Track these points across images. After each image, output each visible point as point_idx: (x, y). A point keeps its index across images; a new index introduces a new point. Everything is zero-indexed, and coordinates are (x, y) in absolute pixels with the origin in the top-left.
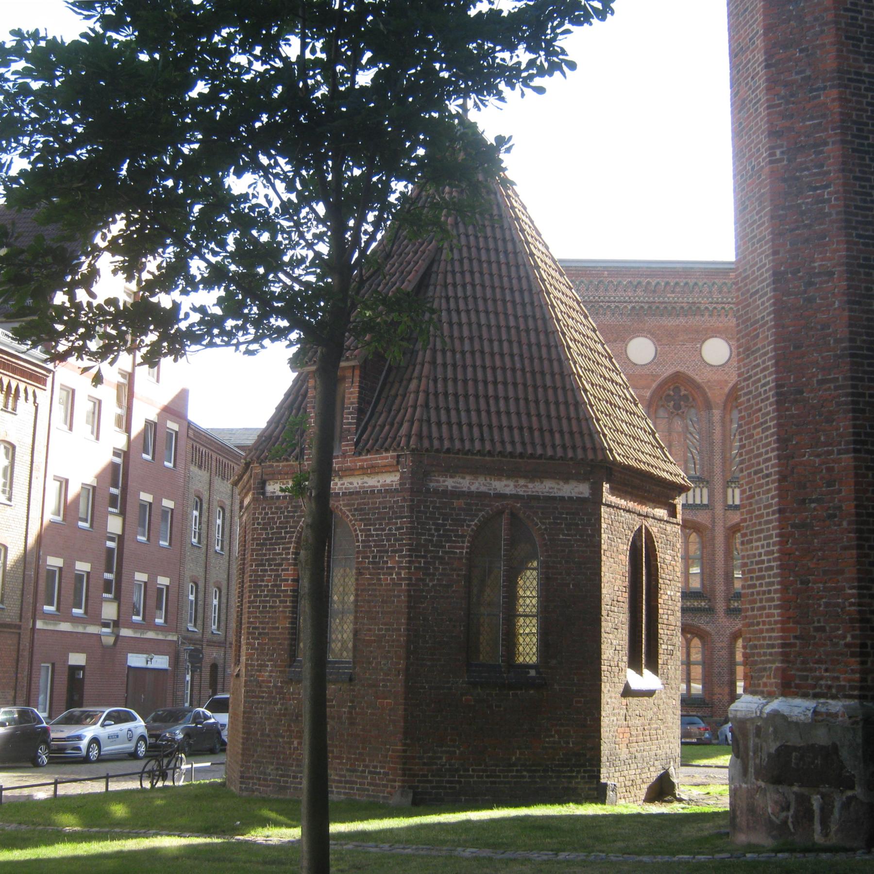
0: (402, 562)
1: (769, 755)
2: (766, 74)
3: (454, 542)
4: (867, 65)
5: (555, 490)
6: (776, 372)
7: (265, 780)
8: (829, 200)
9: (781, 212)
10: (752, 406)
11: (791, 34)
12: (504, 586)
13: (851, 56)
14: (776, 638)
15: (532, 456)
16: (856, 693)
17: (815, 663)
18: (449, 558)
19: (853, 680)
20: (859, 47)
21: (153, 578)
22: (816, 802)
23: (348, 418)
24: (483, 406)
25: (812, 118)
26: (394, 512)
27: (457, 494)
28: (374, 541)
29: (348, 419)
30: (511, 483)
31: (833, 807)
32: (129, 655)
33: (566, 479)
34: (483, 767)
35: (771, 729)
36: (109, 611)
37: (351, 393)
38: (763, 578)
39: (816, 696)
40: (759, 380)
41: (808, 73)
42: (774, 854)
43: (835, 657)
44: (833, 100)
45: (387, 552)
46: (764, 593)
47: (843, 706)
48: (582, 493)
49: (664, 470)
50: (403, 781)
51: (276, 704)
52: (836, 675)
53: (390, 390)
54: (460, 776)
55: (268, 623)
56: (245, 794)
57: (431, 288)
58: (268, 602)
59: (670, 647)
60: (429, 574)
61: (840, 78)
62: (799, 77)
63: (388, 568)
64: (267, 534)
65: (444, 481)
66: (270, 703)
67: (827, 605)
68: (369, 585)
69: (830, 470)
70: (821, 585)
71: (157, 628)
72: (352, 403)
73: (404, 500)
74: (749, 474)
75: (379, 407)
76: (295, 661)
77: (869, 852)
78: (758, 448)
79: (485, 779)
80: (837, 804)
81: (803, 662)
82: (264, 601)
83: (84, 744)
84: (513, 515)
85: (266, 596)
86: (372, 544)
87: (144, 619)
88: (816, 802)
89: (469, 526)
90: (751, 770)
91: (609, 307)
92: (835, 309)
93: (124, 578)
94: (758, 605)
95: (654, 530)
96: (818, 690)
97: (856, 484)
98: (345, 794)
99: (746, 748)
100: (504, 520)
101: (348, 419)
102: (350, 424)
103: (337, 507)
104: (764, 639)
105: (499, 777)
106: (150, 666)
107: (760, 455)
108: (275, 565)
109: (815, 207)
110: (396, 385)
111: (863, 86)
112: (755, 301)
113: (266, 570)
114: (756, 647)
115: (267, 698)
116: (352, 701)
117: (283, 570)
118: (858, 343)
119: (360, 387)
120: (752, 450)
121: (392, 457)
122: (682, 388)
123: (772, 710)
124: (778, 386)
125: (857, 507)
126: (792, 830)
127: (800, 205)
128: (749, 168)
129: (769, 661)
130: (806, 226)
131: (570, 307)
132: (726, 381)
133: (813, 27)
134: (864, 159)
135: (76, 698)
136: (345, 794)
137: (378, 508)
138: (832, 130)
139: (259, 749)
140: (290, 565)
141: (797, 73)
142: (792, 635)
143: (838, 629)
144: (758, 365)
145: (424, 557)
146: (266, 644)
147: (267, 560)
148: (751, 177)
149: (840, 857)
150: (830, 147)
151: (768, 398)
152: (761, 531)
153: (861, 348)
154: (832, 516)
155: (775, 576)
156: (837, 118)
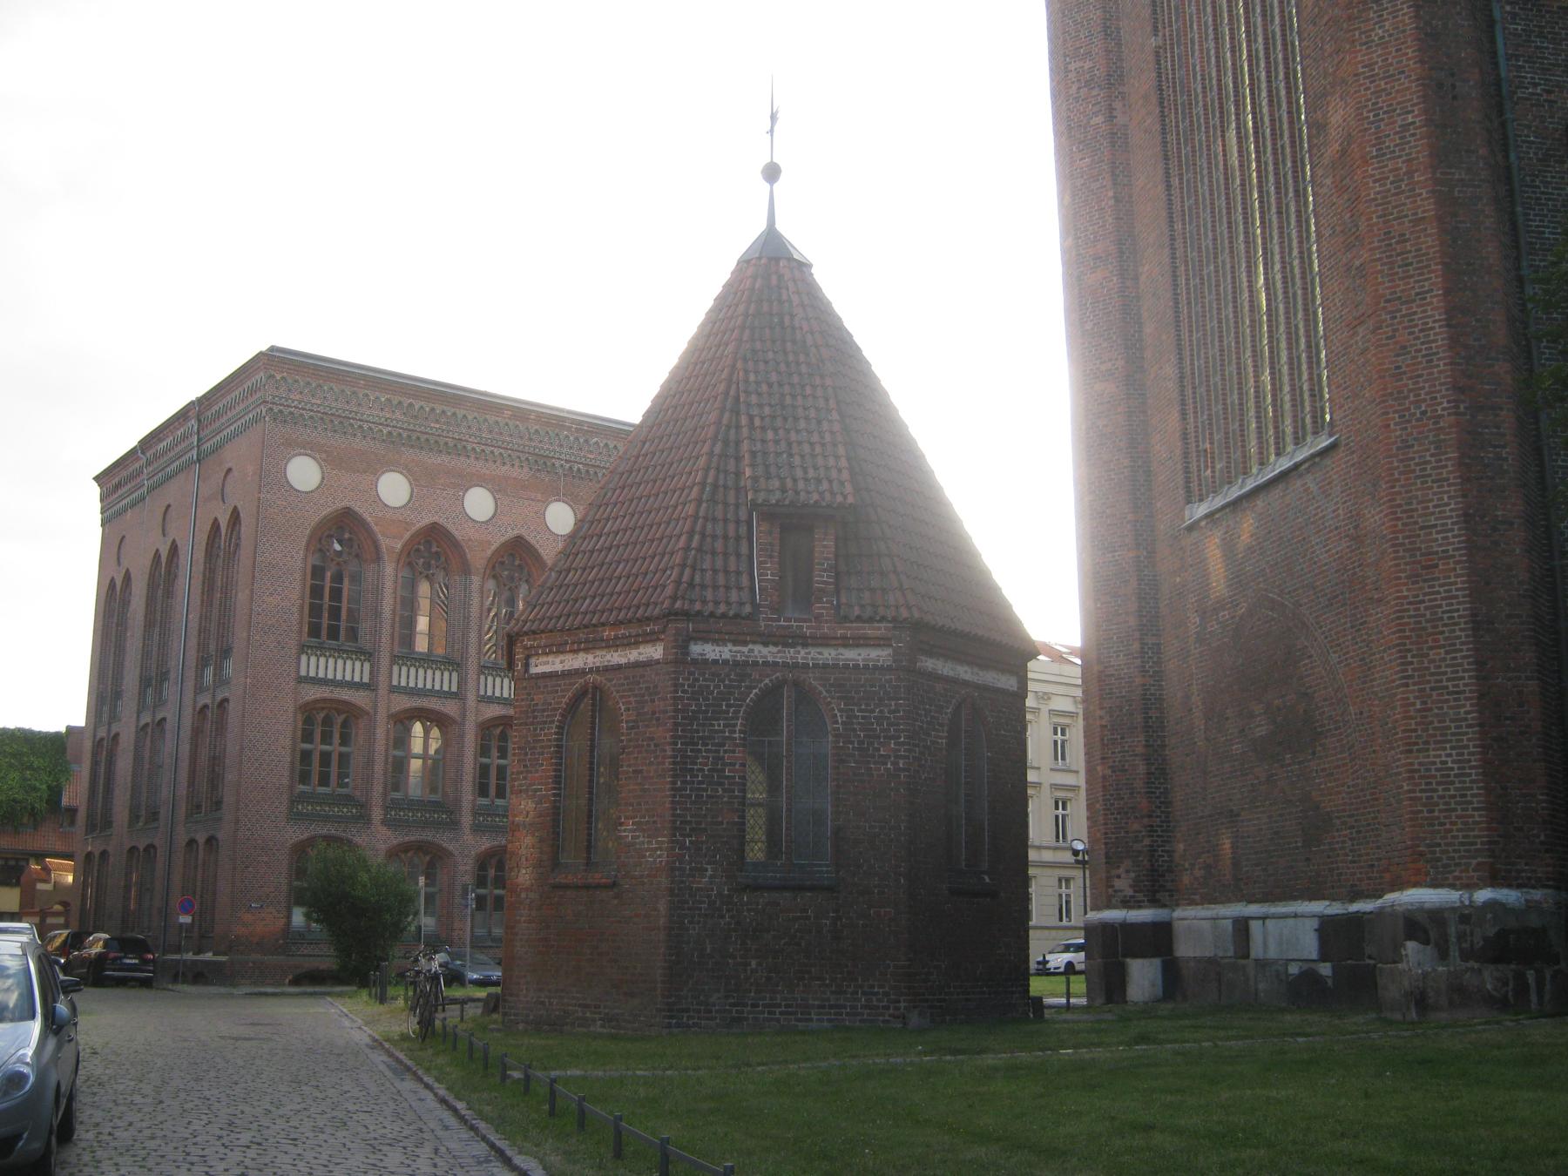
30: (966, 668)
39: (1519, 886)
51: (723, 917)
72: (827, 559)
80: (1548, 977)
85: (700, 783)
88: (1531, 976)
98: (830, 1021)
132: (489, 543)
140: (737, 745)
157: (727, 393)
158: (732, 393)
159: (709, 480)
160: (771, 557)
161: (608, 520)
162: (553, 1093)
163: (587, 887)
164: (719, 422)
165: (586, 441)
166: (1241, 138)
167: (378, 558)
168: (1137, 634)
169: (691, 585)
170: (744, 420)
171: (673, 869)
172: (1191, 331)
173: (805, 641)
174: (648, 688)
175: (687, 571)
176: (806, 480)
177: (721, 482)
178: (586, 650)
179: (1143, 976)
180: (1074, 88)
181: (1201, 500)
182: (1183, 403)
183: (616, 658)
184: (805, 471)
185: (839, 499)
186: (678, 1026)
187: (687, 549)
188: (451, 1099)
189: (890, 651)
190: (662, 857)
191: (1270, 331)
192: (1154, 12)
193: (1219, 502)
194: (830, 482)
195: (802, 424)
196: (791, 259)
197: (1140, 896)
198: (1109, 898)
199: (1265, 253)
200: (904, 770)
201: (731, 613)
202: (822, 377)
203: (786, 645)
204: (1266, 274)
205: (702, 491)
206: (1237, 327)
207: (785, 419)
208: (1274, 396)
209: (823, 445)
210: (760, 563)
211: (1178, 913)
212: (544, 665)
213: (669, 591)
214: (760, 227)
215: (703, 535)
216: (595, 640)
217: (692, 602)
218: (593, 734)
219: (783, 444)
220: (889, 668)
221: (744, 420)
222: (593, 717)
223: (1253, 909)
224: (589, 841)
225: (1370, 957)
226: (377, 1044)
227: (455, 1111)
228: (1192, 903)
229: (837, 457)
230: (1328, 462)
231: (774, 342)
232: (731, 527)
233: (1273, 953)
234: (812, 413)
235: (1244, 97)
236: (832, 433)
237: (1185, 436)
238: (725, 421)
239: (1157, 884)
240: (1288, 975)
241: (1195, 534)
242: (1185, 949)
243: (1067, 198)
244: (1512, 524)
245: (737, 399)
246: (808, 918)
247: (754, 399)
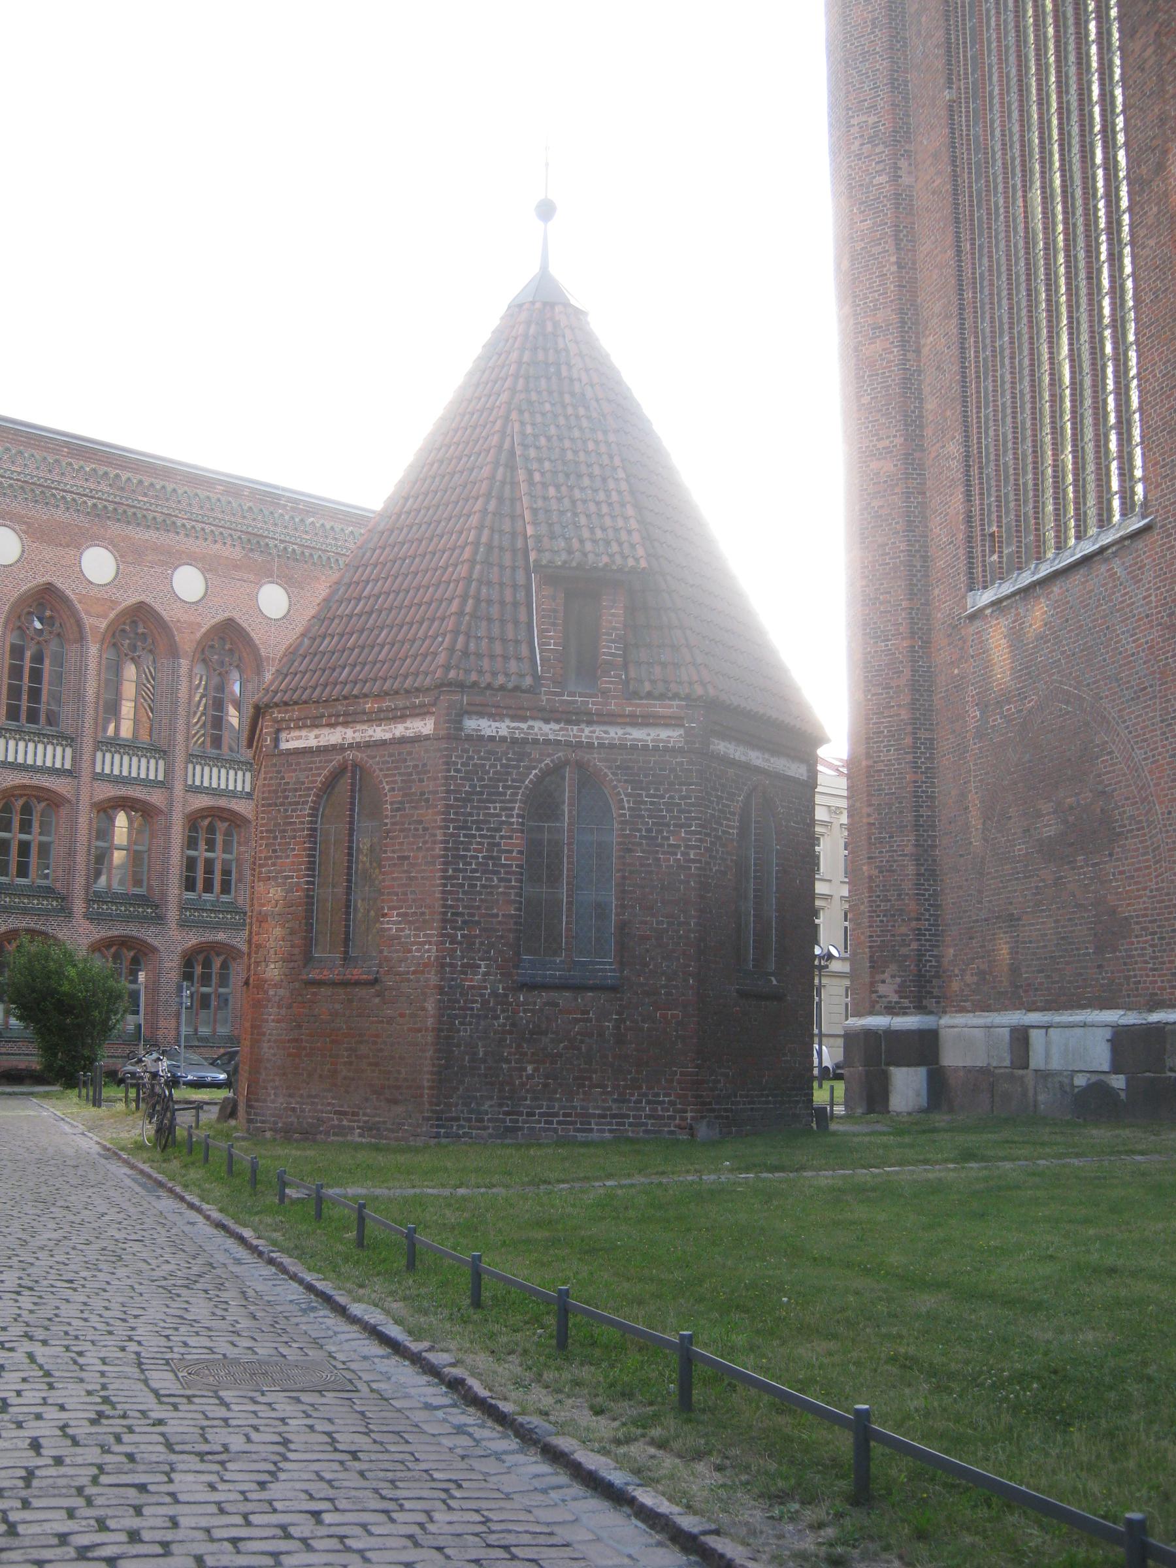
0: (690, 840)
3: (729, 819)
27: (733, 763)
37: (613, 615)
45: (668, 825)
51: (497, 1018)
55: (479, 908)
58: (478, 879)
63: (670, 845)
64: (473, 786)
66: (486, 1017)
68: (642, 865)
72: (615, 629)
82: (471, 878)
85: (475, 871)
86: (646, 814)
89: (738, 802)
91: (63, 498)
98: (611, 1131)
103: (589, 761)
108: (488, 830)
113: (474, 836)
117: (502, 837)
121: (678, 707)
122: (141, 625)
132: (199, 625)
136: (611, 1131)
140: (516, 831)
146: (476, 936)
147: (476, 822)
157: (500, 447)
158: (506, 446)
159: (484, 539)
160: (554, 624)
161: (368, 582)
162: (361, 1219)
163: (345, 984)
164: (492, 477)
165: (302, 520)
166: (1047, 199)
167: (81, 638)
168: (909, 728)
169: (466, 653)
170: (521, 475)
171: (443, 966)
172: (979, 407)
173: (591, 719)
174: (416, 766)
175: (461, 639)
176: (595, 541)
177: (496, 543)
178: (345, 724)
179: (907, 1086)
180: (857, 143)
181: (985, 588)
182: (968, 484)
183: (379, 733)
184: (592, 530)
185: (631, 562)
186: (447, 1136)
187: (460, 613)
188: (230, 1223)
189: (682, 731)
190: (431, 952)
191: (1073, 407)
192: (949, 63)
193: (1007, 588)
194: (620, 544)
195: (586, 482)
196: (567, 305)
197: (906, 1002)
198: (873, 1004)
199: (1070, 322)
200: (694, 861)
201: (510, 685)
202: (605, 432)
203: (569, 722)
204: (1071, 344)
205: (475, 553)
206: (1033, 403)
207: (567, 475)
208: (1076, 475)
209: (610, 504)
210: (541, 632)
211: (945, 1020)
212: (292, 741)
213: (441, 659)
214: (534, 270)
215: (478, 600)
216: (355, 713)
217: (468, 672)
218: (352, 816)
219: (566, 501)
220: (681, 751)
221: (521, 475)
222: (353, 797)
223: (1034, 1018)
224: (347, 933)
225: (1171, 1070)
226: (111, 1153)
227: (241, 1239)
228: (962, 1010)
229: (626, 519)
230: (1140, 544)
231: (550, 393)
232: (508, 593)
233: (1055, 1064)
234: (597, 471)
235: (1051, 154)
236: (620, 492)
237: (969, 519)
238: (499, 476)
239: (924, 990)
240: (1073, 1086)
241: (978, 623)
242: (951, 1058)
243: (846, 264)
245: (512, 453)
246: (589, 1020)
247: (532, 453)
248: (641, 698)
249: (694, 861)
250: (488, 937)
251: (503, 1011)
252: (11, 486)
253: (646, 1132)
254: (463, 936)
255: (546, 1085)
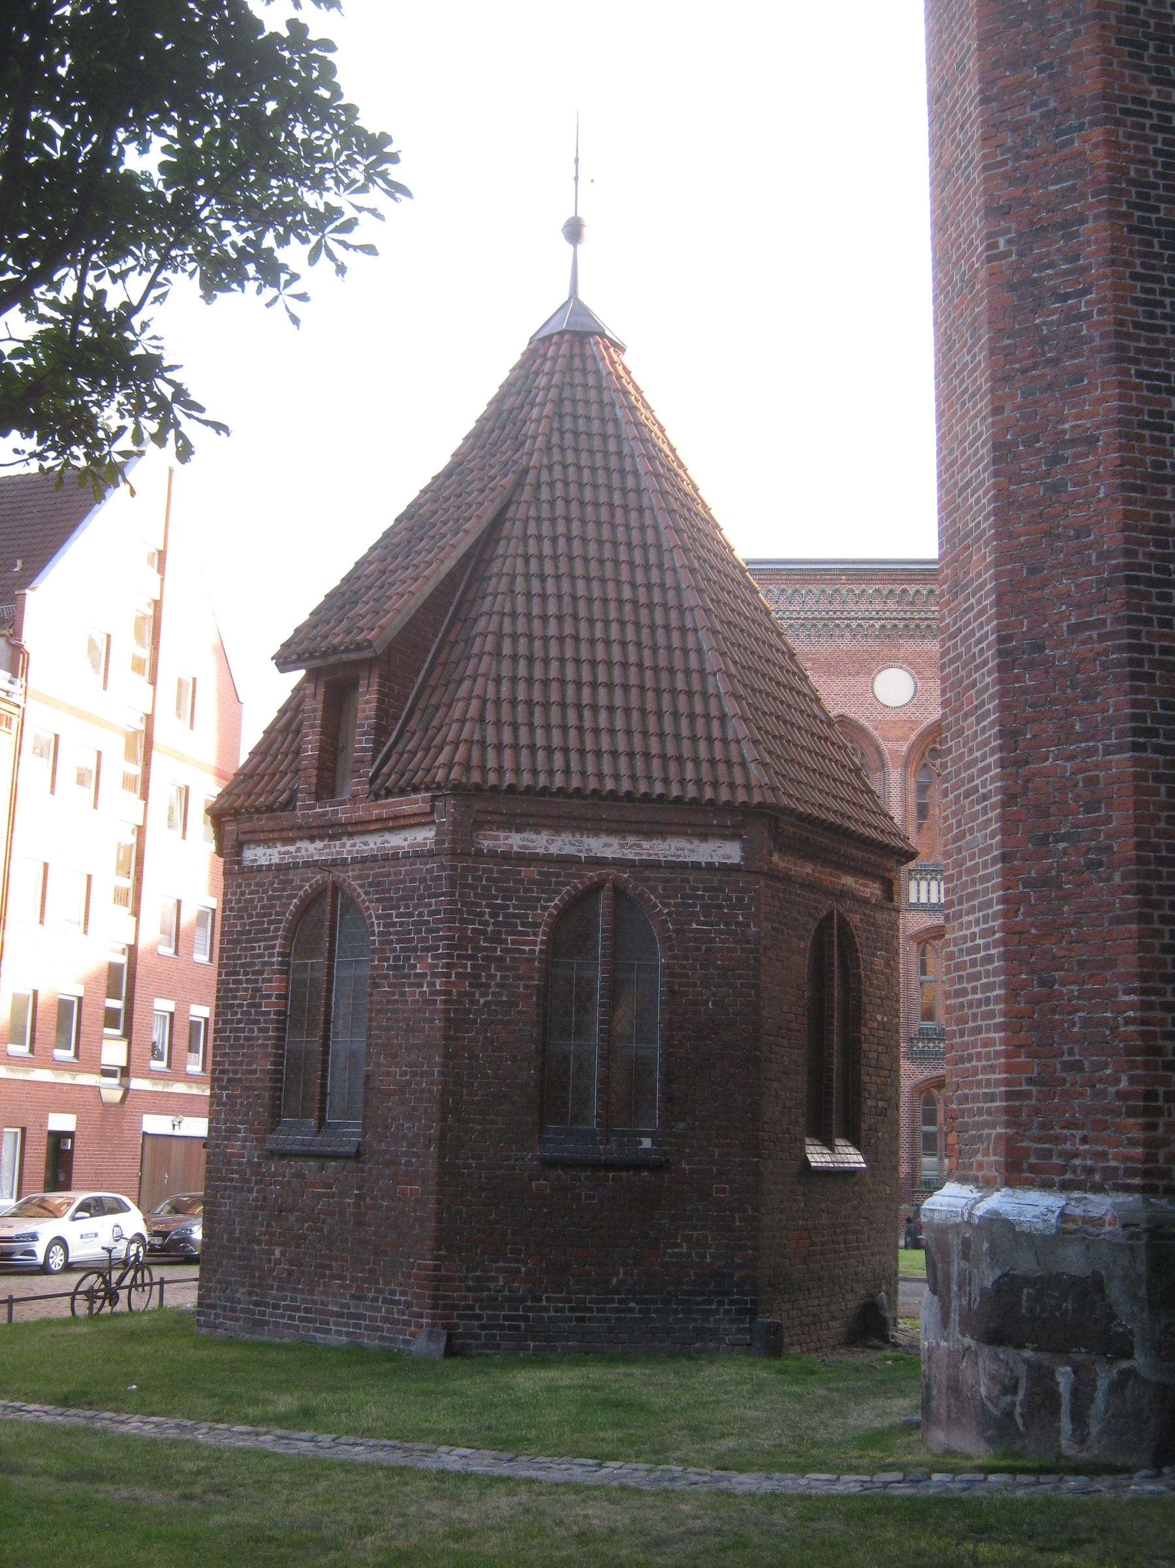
0: (436, 966)
1: (983, 1290)
2: (982, 114)
4: (1154, 88)
5: (686, 852)
6: (999, 615)
7: (234, 1310)
8: (1088, 315)
9: (1008, 342)
10: (961, 680)
11: (1024, 43)
12: (602, 1005)
13: (1127, 72)
14: (998, 1083)
15: (646, 797)
16: (1136, 1181)
17: (1064, 1128)
18: (513, 959)
19: (1130, 1158)
20: (1141, 57)
21: (183, 1005)
22: (1064, 1378)
23: (360, 742)
24: (572, 719)
25: (1059, 179)
26: (427, 888)
28: (397, 933)
29: (360, 742)
30: (615, 841)
31: (1095, 1388)
32: (145, 1116)
33: (704, 837)
34: (564, 1294)
35: (986, 1245)
36: (114, 1053)
37: (367, 702)
38: (975, 977)
39: (1065, 1187)
40: (972, 634)
41: (1052, 104)
42: (981, 1476)
43: (1099, 1116)
44: (1095, 146)
45: (415, 949)
46: (979, 1003)
47: (1114, 1205)
48: (729, 857)
49: (870, 825)
50: (434, 1316)
51: (250, 1190)
52: (1100, 1149)
53: (431, 696)
54: (526, 1309)
55: (241, 1063)
56: (204, 1330)
57: (503, 542)
58: (242, 1030)
59: (880, 1104)
60: (480, 985)
61: (1107, 108)
62: (1036, 113)
63: (416, 975)
64: (243, 925)
65: (506, 838)
67: (1085, 1023)
68: (388, 1002)
69: (1091, 782)
70: (1075, 987)
71: (190, 1079)
72: (367, 718)
73: (442, 867)
74: (957, 797)
75: (412, 725)
76: (279, 1123)
77: (1158, 1475)
78: (971, 751)
79: (567, 1313)
80: (1102, 1384)
81: (1043, 1126)
83: (40, 1248)
84: (616, 889)
85: (239, 1021)
87: (169, 1065)
88: (1064, 1378)
89: (544, 908)
90: (955, 1317)
91: (848, 626)
92: (1100, 500)
93: (137, 1007)
94: (971, 1024)
95: (855, 919)
96: (1067, 1176)
97: (1137, 805)
98: (348, 1334)
99: (948, 1278)
100: (604, 901)
101: (360, 742)
102: (363, 750)
104: (979, 1084)
105: (591, 1310)
106: (177, 1132)
107: (974, 763)
108: (254, 973)
109: (1064, 328)
110: (441, 690)
111: (1148, 123)
112: (966, 499)
113: (239, 982)
114: (965, 1099)
115: (238, 1181)
116: (360, 1188)
117: (264, 981)
118: (1141, 559)
119: (380, 692)
120: (962, 755)
121: (424, 800)
123: (988, 1212)
124: (1001, 640)
125: (1138, 846)
126: (1022, 1429)
127: (1038, 328)
128: (957, 278)
129: (985, 1125)
130: (1049, 361)
131: (726, 576)
133: (1061, 27)
134: (1150, 244)
135: (62, 1178)
136: (348, 1334)
137: (403, 881)
138: (1095, 194)
139: (225, 1261)
140: (274, 972)
141: (1034, 108)
142: (1024, 1076)
143: (1106, 1066)
144: (971, 608)
145: (472, 958)
146: (237, 1097)
147: (243, 965)
148: (960, 293)
149: (1103, 1485)
150: (1090, 225)
151: (985, 663)
152: (974, 895)
153: (1147, 568)
154: (1092, 865)
155: (996, 972)
156: (1102, 175)
160: (312, 726)
167: (883, 765)
200: (439, 993)
220: (431, 854)
244: (1091, 441)
248: (387, 797)
249: (439, 993)
250: (248, 1097)
251: (256, 1183)
252: (791, 626)
253: (382, 1338)
254: (228, 1096)
255: (290, 1272)
